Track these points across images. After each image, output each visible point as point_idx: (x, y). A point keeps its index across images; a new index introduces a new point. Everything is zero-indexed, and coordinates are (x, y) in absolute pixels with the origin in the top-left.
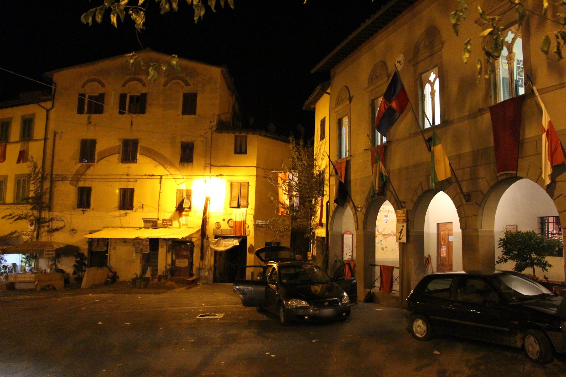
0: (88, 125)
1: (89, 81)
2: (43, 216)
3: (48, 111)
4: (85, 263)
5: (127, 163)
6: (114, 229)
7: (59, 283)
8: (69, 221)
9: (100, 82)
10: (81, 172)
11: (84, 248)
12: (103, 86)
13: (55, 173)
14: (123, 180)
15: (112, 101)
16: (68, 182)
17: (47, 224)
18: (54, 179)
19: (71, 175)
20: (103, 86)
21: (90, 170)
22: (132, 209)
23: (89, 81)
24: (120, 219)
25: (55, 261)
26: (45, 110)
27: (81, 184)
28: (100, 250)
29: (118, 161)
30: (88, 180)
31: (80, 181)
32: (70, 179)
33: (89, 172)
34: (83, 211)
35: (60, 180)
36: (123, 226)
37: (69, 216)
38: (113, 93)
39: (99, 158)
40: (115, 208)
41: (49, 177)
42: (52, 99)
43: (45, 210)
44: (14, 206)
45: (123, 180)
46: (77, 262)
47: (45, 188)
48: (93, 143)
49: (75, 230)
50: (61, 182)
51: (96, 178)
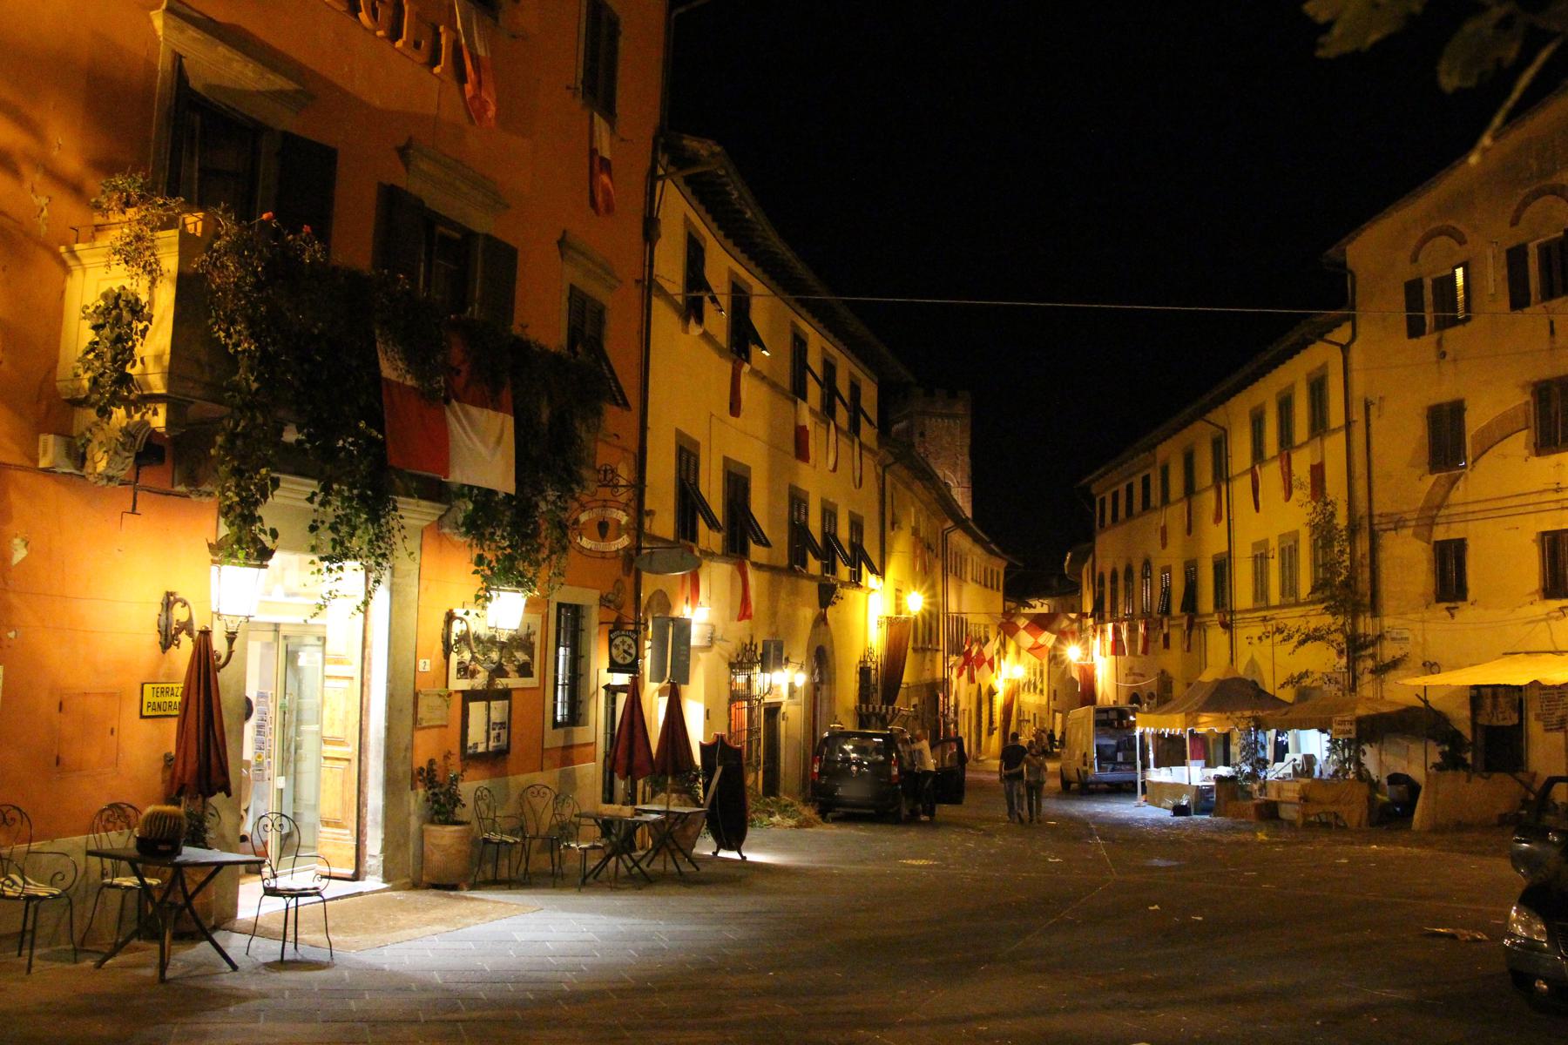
0: (1438, 362)
1: (1424, 241)
2: (1361, 630)
3: (1345, 349)
4: (1465, 760)
5: (1553, 453)
6: (1533, 658)
7: (1355, 813)
8: (1420, 639)
9: (1451, 233)
10: (1438, 500)
11: (1461, 716)
13: (1376, 512)
14: (1547, 506)
15: (1491, 278)
16: (1410, 531)
17: (1370, 651)
18: (1376, 528)
19: (1415, 510)
20: (1462, 241)
21: (1458, 489)
23: (1424, 241)
24: (1549, 625)
25: (1358, 750)
26: (1338, 349)
27: (1440, 534)
28: (1502, 723)
29: (1526, 453)
30: (1456, 518)
31: (1437, 524)
32: (1413, 523)
33: (1456, 495)
34: (1448, 609)
35: (1391, 529)
36: (1560, 649)
37: (1419, 626)
38: (1489, 253)
39: (1479, 451)
40: (1531, 594)
41: (1366, 523)
42: (1352, 319)
43: (1364, 612)
44: (1312, 607)
45: (1547, 506)
46: (1443, 754)
47: (1359, 554)
49: (1436, 664)
50: (1393, 532)
51: (1473, 512)
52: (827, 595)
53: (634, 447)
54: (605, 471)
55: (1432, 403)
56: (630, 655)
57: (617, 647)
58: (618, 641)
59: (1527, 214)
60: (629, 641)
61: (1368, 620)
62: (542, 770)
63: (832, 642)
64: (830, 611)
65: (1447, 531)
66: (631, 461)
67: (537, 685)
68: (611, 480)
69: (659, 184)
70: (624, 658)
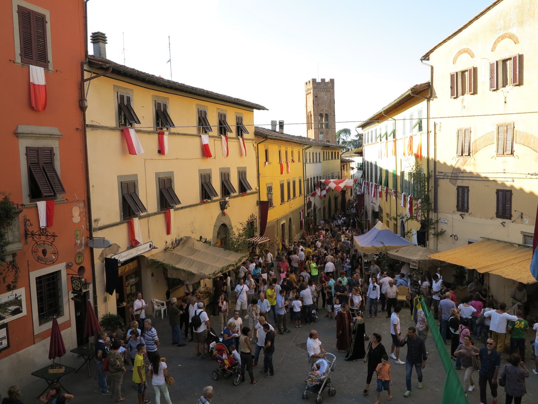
12: (472, 56)
13: (437, 170)
22: (510, 219)
27: (460, 183)
34: (461, 215)
41: (433, 175)
48: (467, 132)
49: (456, 235)
52: (223, 206)
53: (84, 197)
55: (459, 127)
56: (79, 287)
57: (74, 284)
58: (74, 282)
59: (499, 45)
60: (78, 282)
61: (433, 213)
62: (34, 344)
63: (230, 221)
64: (225, 210)
65: (462, 182)
68: (45, 233)
69: (86, 84)
70: (77, 288)
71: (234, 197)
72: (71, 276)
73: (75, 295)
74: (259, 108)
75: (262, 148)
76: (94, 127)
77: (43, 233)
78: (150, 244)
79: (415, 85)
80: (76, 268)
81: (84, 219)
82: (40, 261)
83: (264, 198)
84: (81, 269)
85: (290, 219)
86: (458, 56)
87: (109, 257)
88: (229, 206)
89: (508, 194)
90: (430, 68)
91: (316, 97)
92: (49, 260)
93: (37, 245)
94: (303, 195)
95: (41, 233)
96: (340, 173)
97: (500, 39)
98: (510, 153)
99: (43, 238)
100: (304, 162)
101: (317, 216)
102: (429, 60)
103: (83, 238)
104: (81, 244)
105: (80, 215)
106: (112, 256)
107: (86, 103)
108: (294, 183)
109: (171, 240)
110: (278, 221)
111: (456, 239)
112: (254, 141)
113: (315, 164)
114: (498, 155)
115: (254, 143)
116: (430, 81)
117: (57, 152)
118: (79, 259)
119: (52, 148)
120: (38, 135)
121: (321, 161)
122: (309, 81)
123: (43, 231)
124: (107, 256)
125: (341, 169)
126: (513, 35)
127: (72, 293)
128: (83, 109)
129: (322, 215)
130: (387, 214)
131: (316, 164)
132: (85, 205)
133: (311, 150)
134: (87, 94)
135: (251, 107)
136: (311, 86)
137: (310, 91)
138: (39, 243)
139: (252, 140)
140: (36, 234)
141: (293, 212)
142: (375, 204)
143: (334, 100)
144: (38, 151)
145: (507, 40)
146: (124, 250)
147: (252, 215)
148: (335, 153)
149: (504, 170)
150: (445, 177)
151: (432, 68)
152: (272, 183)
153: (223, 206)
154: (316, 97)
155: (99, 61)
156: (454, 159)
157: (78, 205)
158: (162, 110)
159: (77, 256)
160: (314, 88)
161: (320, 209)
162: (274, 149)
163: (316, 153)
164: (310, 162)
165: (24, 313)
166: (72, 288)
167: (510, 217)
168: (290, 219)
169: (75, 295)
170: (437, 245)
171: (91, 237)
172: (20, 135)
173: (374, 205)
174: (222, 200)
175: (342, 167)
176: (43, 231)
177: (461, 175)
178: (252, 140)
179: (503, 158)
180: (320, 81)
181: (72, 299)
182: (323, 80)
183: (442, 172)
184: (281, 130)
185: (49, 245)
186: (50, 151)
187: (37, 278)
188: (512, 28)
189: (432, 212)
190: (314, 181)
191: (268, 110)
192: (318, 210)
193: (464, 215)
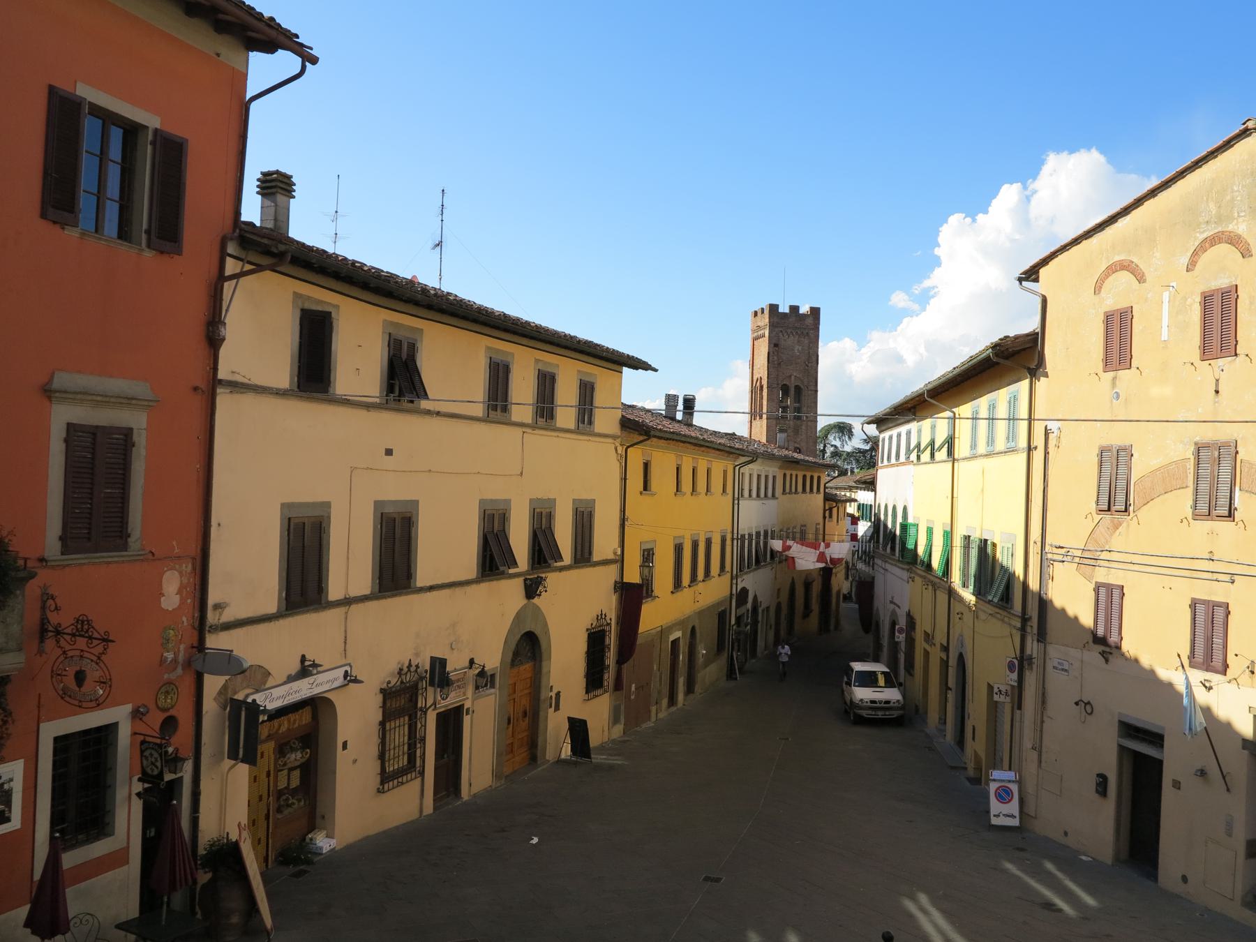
12: (1141, 279)
27: (1102, 576)
33: (1117, 542)
49: (1089, 703)
52: (532, 589)
53: (194, 548)
54: (83, 622)
55: (1105, 443)
56: (157, 768)
58: (147, 753)
59: (1205, 258)
60: (156, 755)
61: (1035, 642)
63: (546, 625)
66: (187, 567)
67: (18, 826)
68: (87, 631)
69: (228, 287)
71: (562, 569)
72: (142, 738)
73: (146, 785)
74: (637, 364)
75: (636, 457)
76: (235, 386)
77: (82, 630)
78: (346, 672)
79: (1002, 336)
80: (156, 719)
81: (189, 601)
82: (67, 699)
83: (633, 576)
84: (170, 724)
85: (693, 629)
86: (1107, 276)
87: (240, 696)
88: (546, 591)
89: (1219, 613)
90: (1039, 300)
91: (775, 346)
92: (88, 698)
93: (66, 658)
94: (729, 575)
95: (77, 630)
96: (821, 527)
97: (1207, 245)
98: (1226, 513)
99: (81, 642)
100: (736, 496)
101: (759, 625)
102: (1038, 282)
103: (182, 647)
104: (175, 660)
105: (179, 592)
106: (247, 696)
107: (223, 329)
108: (709, 542)
109: (399, 663)
110: (663, 632)
111: (1089, 712)
112: (619, 440)
113: (761, 502)
114: (1196, 516)
115: (618, 444)
116: (1038, 330)
117: (140, 439)
118: (166, 698)
119: (131, 430)
120: (99, 398)
121: (777, 495)
122: (763, 309)
123: (82, 626)
124: (235, 693)
125: (824, 517)
126: (1239, 237)
127: (140, 780)
128: (214, 341)
129: (773, 621)
130: (926, 634)
131: (764, 502)
132: (194, 569)
133: (755, 468)
134: (227, 311)
135: (617, 361)
136: (765, 320)
137: (762, 332)
138: (70, 654)
139: (614, 437)
140: (65, 631)
141: (701, 613)
142: (899, 607)
143: (818, 356)
144: (94, 434)
145: (1224, 248)
146: (280, 682)
147: (602, 614)
148: (812, 478)
149: (1211, 552)
150: (1065, 559)
151: (1044, 301)
152: (655, 541)
153: (532, 589)
154: (776, 345)
155: (263, 237)
156: (1089, 516)
157: (177, 566)
158: (404, 356)
159: (163, 690)
160: (772, 326)
161: (768, 608)
162: (664, 460)
163: (767, 477)
164: (750, 496)
165: (15, 823)
166: (138, 768)
167: (1224, 669)
168: (693, 629)
169: (146, 785)
170: (1042, 722)
171: (200, 646)
172: (57, 394)
173: (897, 608)
174: (530, 575)
175: (827, 512)
176: (82, 626)
177: (1104, 555)
178: (614, 437)
179: (1207, 525)
180: (787, 311)
181: (138, 795)
182: (794, 309)
183: (1062, 548)
184: (688, 416)
185: (92, 661)
186: (126, 435)
187: (56, 739)
188: (1235, 221)
189: (1033, 640)
190: (758, 543)
191: (656, 370)
192: (763, 611)
193: (1111, 653)
